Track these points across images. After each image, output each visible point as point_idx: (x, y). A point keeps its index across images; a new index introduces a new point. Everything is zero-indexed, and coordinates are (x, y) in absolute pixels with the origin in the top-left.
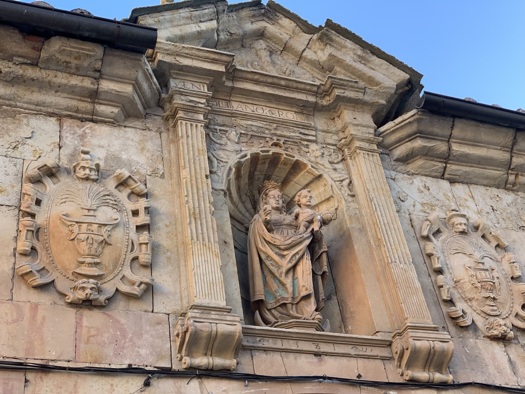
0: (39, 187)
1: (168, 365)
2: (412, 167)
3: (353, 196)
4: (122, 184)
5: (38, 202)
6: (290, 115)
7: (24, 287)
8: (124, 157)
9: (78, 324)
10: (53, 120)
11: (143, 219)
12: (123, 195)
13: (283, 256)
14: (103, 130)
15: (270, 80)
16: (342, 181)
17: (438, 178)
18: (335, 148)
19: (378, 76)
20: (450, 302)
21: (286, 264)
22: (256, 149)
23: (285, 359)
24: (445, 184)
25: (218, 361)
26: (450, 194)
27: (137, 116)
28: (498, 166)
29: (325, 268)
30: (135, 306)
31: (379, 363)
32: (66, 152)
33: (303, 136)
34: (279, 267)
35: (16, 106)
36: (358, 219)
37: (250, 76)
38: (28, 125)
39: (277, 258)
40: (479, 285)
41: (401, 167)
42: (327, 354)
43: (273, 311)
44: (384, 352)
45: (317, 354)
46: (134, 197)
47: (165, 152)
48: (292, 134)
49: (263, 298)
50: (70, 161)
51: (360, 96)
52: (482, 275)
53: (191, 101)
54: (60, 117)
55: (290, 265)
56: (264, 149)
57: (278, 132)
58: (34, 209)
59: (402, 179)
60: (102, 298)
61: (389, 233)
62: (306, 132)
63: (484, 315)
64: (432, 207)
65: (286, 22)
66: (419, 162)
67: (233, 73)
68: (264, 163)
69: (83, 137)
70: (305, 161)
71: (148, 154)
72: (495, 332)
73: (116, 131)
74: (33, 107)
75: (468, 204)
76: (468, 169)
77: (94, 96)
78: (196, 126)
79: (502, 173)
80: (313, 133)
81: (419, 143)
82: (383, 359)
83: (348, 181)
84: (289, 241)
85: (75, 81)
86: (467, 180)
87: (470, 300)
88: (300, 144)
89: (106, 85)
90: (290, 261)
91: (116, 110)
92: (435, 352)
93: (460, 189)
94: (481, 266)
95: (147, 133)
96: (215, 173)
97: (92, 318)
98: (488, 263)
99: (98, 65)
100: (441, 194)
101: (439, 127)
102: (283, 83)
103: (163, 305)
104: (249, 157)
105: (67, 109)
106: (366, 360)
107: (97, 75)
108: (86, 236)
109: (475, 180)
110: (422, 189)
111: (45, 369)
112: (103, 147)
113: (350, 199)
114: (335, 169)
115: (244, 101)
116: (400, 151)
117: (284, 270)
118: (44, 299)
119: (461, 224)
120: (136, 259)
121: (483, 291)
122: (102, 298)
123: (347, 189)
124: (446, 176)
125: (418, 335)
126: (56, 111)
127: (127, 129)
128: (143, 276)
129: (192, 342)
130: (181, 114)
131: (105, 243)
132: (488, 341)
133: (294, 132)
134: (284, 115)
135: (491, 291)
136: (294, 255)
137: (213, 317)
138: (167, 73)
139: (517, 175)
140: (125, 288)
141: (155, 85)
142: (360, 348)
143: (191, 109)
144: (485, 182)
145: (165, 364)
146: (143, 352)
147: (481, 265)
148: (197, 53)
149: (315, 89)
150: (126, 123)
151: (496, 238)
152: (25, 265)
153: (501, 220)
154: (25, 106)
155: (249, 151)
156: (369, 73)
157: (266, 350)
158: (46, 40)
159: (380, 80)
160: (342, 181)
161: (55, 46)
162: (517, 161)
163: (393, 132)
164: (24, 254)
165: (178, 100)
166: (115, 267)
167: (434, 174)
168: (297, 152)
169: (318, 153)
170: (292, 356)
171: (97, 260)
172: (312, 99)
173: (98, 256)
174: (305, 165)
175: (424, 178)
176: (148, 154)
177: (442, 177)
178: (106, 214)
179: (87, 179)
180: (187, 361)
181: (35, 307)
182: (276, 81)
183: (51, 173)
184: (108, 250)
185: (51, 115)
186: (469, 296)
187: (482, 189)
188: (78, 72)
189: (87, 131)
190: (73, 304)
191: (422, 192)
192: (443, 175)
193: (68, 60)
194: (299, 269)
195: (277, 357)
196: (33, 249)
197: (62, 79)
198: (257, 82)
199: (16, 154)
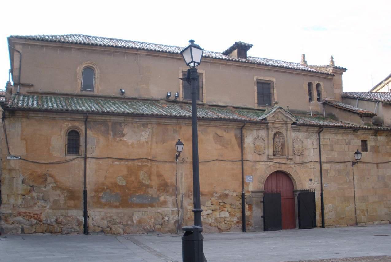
4: (263, 139)
6: (281, 125)
12: (263, 141)
14: (260, 131)
20: (294, 151)
21: (278, 147)
24: (298, 132)
44: (286, 158)
65: (283, 110)
67: (275, 121)
86: (301, 132)
97: (260, 156)
101: (299, 127)
111: (257, 161)
156: (292, 119)
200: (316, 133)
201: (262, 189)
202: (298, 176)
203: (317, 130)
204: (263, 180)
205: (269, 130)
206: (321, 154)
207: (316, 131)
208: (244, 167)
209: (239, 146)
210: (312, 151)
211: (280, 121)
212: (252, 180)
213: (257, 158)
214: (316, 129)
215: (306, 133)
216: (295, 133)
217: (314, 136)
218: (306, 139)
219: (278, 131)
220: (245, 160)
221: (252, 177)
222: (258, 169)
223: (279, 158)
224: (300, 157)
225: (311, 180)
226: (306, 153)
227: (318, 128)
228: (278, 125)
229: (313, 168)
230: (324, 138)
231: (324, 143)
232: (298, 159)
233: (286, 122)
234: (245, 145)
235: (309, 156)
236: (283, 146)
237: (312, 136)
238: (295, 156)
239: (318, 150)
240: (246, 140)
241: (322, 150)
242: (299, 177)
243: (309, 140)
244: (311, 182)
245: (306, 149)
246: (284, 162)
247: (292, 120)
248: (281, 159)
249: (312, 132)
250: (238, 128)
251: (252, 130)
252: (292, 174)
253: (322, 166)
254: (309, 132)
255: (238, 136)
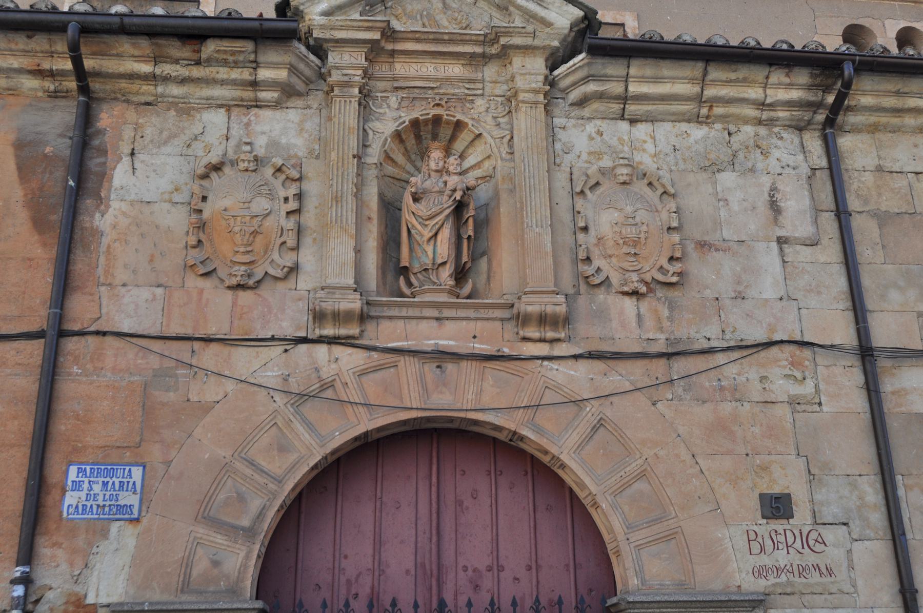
0: (205, 183)
1: (305, 335)
2: (586, 112)
3: (512, 153)
5: (204, 198)
6: (456, 70)
7: (193, 276)
8: (284, 141)
9: (234, 304)
10: (222, 111)
11: (293, 205)
12: (277, 183)
13: (426, 226)
14: (266, 113)
15: (431, 37)
16: (502, 138)
17: (616, 119)
18: (503, 99)
19: (551, 15)
20: (588, 260)
21: (427, 234)
22: (415, 115)
23: (407, 325)
24: (624, 126)
25: (343, 332)
26: (626, 138)
27: (299, 95)
28: (686, 100)
29: (471, 233)
30: (280, 286)
31: (498, 324)
32: (232, 142)
33: (467, 91)
34: (422, 235)
35: (190, 103)
36: (511, 179)
37: (410, 36)
38: (200, 121)
39: (419, 227)
40: (621, 242)
41: (576, 112)
42: (447, 319)
43: (419, 275)
44: (506, 314)
45: (437, 319)
46: (288, 183)
47: (322, 130)
48: (457, 91)
49: (407, 265)
50: (235, 152)
51: (529, 41)
52: (629, 231)
53: (346, 75)
54: (228, 108)
55: (431, 234)
56: (424, 112)
57: (442, 91)
58: (201, 205)
59: (574, 126)
60: (251, 282)
61: (533, 196)
62: (472, 86)
63: (621, 271)
64: (599, 155)
66: (596, 105)
68: (426, 125)
69: (248, 125)
70: (466, 120)
71: (306, 135)
72: (626, 289)
73: (278, 114)
74: (204, 101)
75: (646, 146)
76: (650, 108)
77: (254, 84)
78: (350, 102)
79: (692, 107)
80: (480, 86)
81: (592, 87)
82: (502, 320)
83: (508, 137)
84: (430, 213)
85: (235, 74)
86: (651, 119)
87: (610, 256)
88: (465, 100)
89: (264, 74)
90: (430, 231)
91: (276, 95)
92: (546, 314)
93: (642, 130)
94: (631, 221)
95: (308, 111)
96: (369, 146)
97: (245, 297)
98: (642, 216)
99: (252, 57)
100: (615, 139)
101: (614, 68)
102: (446, 37)
103: (305, 282)
104: (407, 123)
105: (233, 100)
106: (485, 323)
107: (254, 65)
108: (239, 228)
109: (660, 117)
110: (594, 135)
111: (208, 340)
112: (265, 133)
113: (509, 157)
114: (498, 125)
115: (408, 60)
116: (574, 95)
117: (425, 239)
118: (207, 284)
119: (622, 175)
120: (284, 243)
121: (625, 247)
122: (251, 282)
123: (506, 146)
124: (626, 117)
125: (531, 300)
126: (224, 102)
127: (289, 110)
128: (288, 260)
129: (319, 317)
130: (337, 91)
131: (255, 233)
132: (621, 296)
133: (459, 88)
134: (450, 70)
135: (635, 246)
136: (434, 225)
137: (337, 296)
138: (325, 46)
139: (711, 107)
140: (272, 271)
141: (312, 62)
142: (482, 311)
143: (347, 85)
144: (673, 118)
145: (303, 334)
146: (284, 324)
147: (630, 220)
148: (349, 23)
149: (482, 38)
150: (289, 104)
151: (663, 186)
152: (195, 255)
153: (680, 162)
154: (198, 101)
155: (407, 117)
157: (390, 318)
158: (201, 44)
159: (552, 20)
160: (502, 138)
161: (210, 48)
162: (710, 92)
163: (567, 75)
164: (194, 247)
165: (336, 77)
166: (266, 252)
167: (612, 116)
168: (459, 109)
169: (483, 109)
170: (414, 322)
171: (249, 249)
172: (478, 50)
173: (250, 245)
174: (467, 124)
175: (599, 122)
176: (306, 135)
177: (622, 118)
178: (261, 205)
179: (247, 170)
180: (318, 332)
181: (201, 292)
182: (438, 36)
183: (217, 168)
184: (259, 238)
185: (220, 106)
186: (610, 252)
187: (668, 126)
188: (236, 65)
189: (253, 118)
190: (229, 288)
191: (593, 139)
192: (623, 116)
193: (225, 57)
194: (439, 237)
195: (401, 323)
196: (199, 241)
197: (223, 73)
198: (418, 40)
199: (190, 152)
200: (800, 128)
201: (234, 591)
202: (634, 466)
203: (795, 94)
204: (255, 505)
205: (336, 108)
206: (866, 281)
207: (790, 104)
208: (67, 388)
209: (39, 224)
210: (768, 257)
211: (438, 39)
212: (133, 500)
213: (218, 309)
214: (788, 89)
215: (698, 132)
216: (591, 128)
217: (776, 153)
218: (703, 169)
219: (437, 120)
220: (81, 334)
221: (137, 473)
222: (206, 408)
223: (434, 313)
224: (644, 305)
225: (777, 507)
226: (711, 275)
227: (802, 76)
228: (429, 68)
229: (794, 402)
230: (879, 169)
231: (889, 203)
232: (625, 321)
233: (491, 37)
234: (108, 220)
235: (740, 297)
236: (469, 218)
237: (765, 154)
238: (601, 296)
239: (831, 252)
240: (120, 175)
241: (866, 253)
242: (642, 475)
243: (727, 179)
244: (779, 525)
245: (703, 246)
246: (480, 347)
247: (548, 24)
248: (450, 326)
249: (760, 122)
250: (55, 95)
251: (185, 110)
252: (563, 443)
253: (888, 386)
254: (723, 118)
255: (48, 150)
